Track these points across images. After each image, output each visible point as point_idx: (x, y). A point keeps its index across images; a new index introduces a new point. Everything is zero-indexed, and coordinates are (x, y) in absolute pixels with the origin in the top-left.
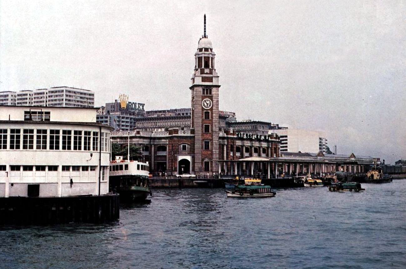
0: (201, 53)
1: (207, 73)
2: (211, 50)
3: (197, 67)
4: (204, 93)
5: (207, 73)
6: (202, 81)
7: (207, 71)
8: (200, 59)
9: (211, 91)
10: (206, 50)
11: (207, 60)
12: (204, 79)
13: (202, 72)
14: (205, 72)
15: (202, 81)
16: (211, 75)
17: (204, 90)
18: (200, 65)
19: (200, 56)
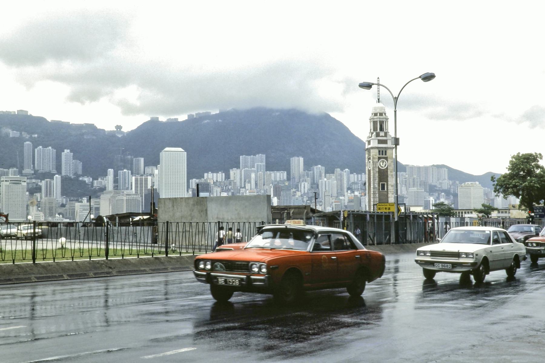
0: (376, 117)
1: (382, 136)
2: (385, 114)
3: (372, 131)
4: (379, 154)
5: (382, 136)
6: (379, 143)
7: (382, 134)
8: (375, 123)
9: (386, 152)
10: (381, 114)
11: (381, 123)
12: (380, 142)
13: (378, 135)
14: (381, 135)
15: (379, 143)
16: (385, 138)
17: (379, 151)
18: (375, 129)
19: (376, 120)
